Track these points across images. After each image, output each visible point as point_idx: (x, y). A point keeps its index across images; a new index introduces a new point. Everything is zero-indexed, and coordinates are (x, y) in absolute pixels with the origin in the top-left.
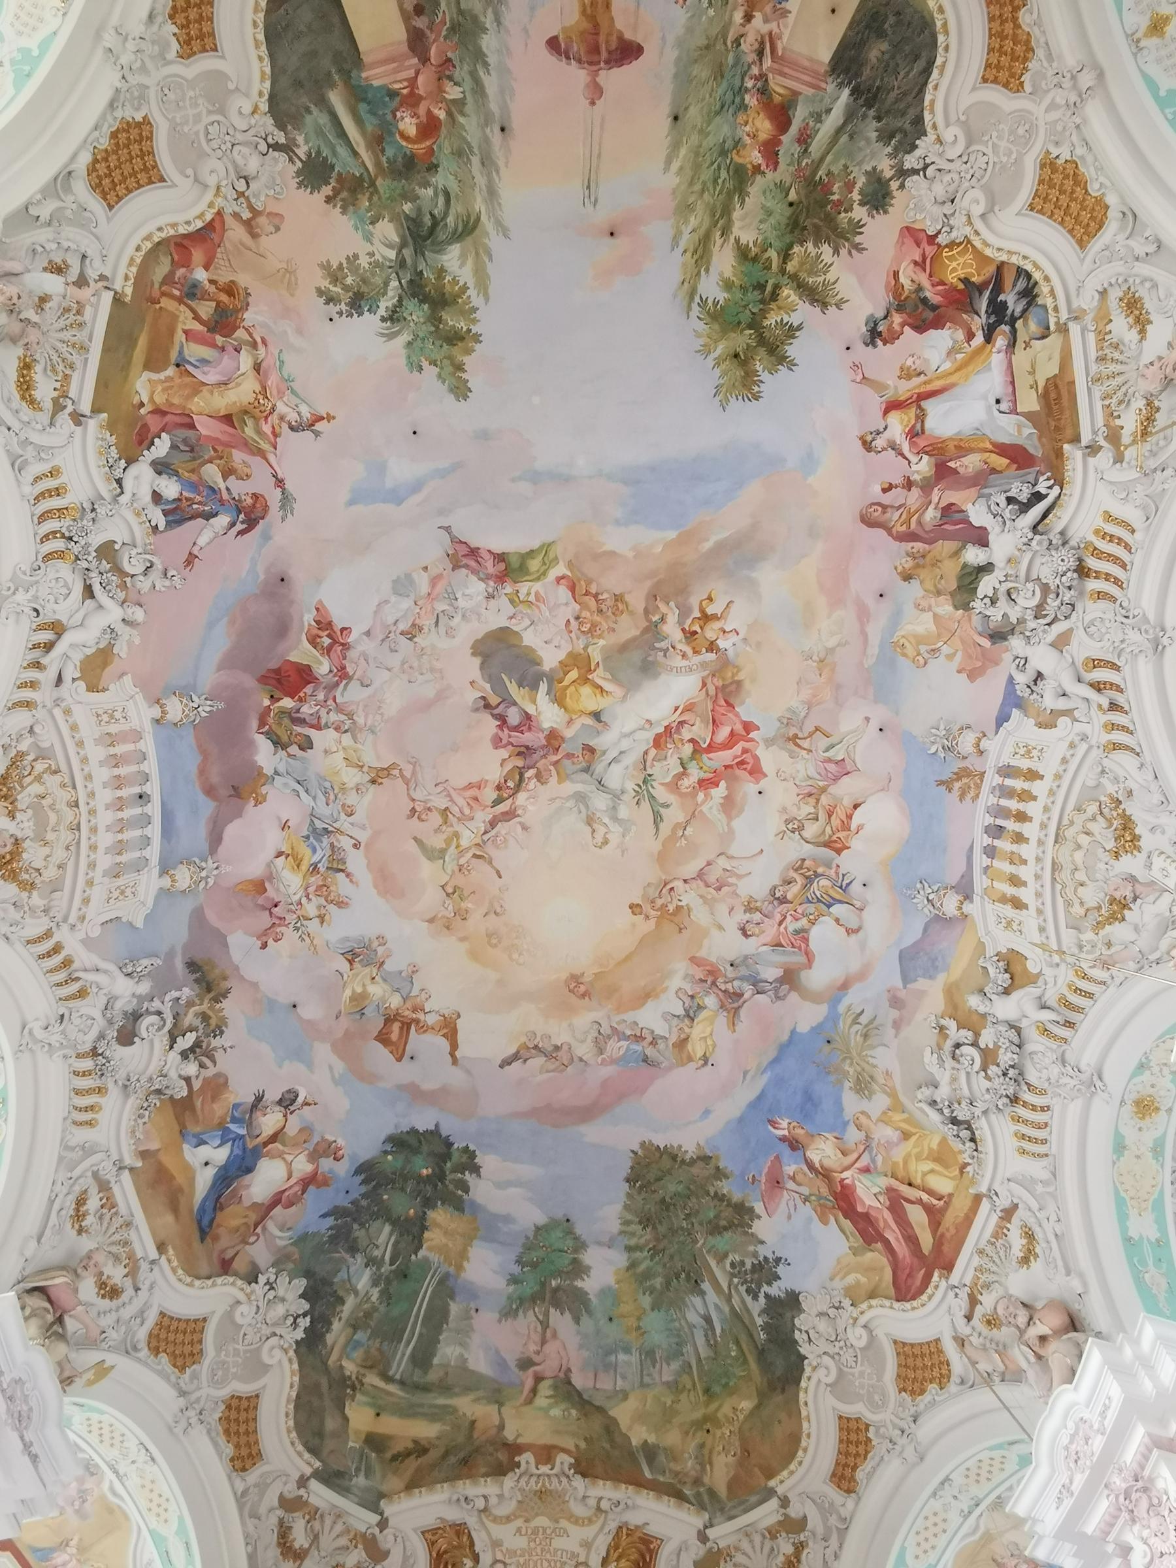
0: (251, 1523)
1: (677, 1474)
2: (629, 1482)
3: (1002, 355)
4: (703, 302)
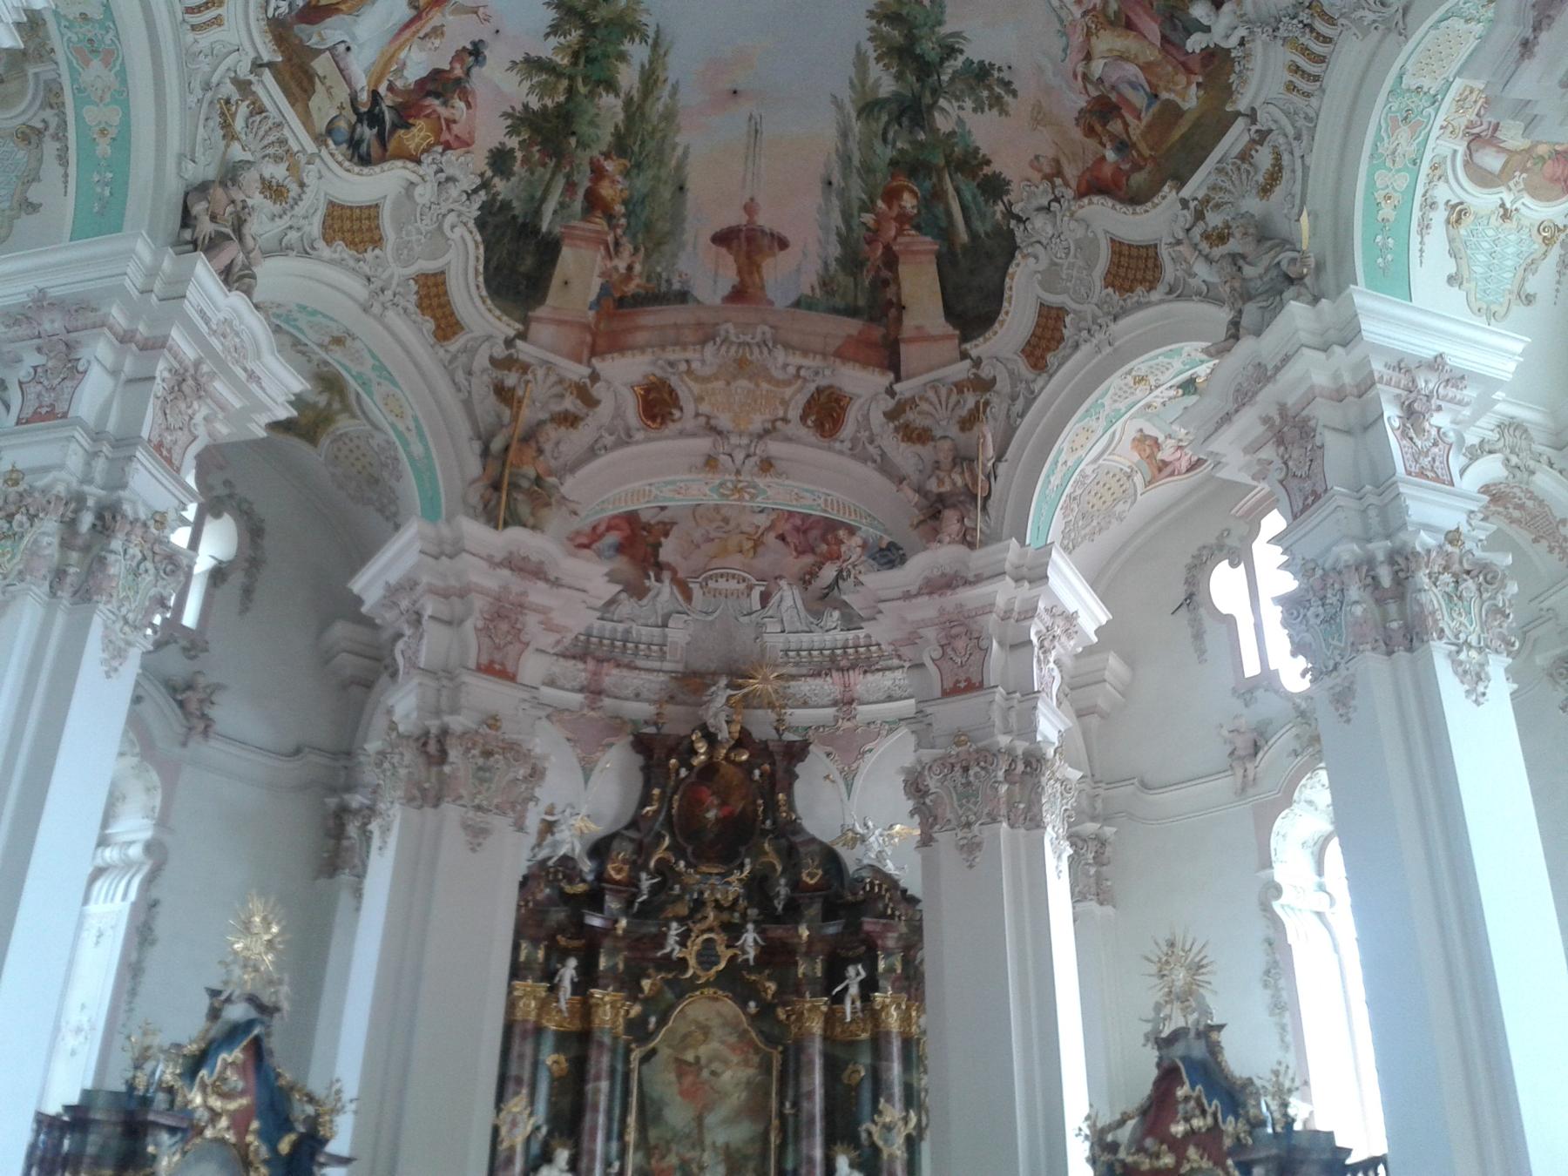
3: (359, 87)
4: (644, 38)
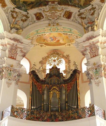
0: (7, 14)
1: (75, 3)
2: (67, 5)
